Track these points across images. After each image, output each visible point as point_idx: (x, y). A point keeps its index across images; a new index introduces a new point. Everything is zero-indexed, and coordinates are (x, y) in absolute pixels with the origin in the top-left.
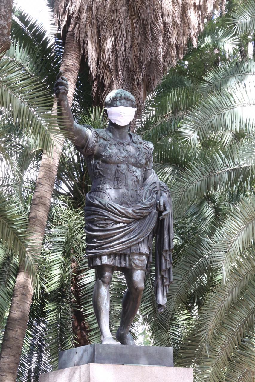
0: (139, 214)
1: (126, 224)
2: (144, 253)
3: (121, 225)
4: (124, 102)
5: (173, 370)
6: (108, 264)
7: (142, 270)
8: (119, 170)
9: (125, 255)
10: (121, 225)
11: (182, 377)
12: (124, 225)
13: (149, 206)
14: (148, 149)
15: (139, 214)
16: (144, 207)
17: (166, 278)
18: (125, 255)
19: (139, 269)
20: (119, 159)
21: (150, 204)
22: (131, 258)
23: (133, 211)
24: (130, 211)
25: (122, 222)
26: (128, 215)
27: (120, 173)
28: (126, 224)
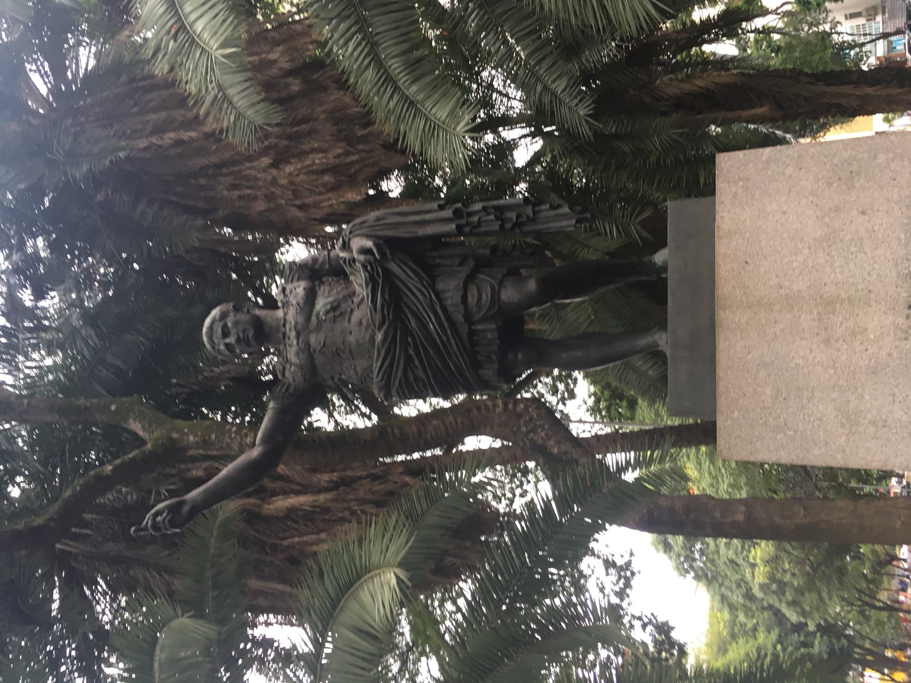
0: (386, 313)
1: (410, 340)
2: (462, 292)
3: (411, 352)
4: (217, 338)
5: (724, 214)
6: (496, 366)
7: (499, 290)
8: (319, 351)
9: (472, 333)
10: (411, 352)
11: (741, 183)
12: (412, 344)
13: (370, 287)
14: (293, 273)
15: (386, 313)
16: (372, 302)
17: (518, 216)
18: (472, 333)
19: (499, 298)
20: (301, 353)
21: (367, 286)
22: (477, 318)
23: (379, 329)
24: (379, 337)
25: (407, 351)
26: (389, 339)
27: (324, 349)
28: (410, 340)
